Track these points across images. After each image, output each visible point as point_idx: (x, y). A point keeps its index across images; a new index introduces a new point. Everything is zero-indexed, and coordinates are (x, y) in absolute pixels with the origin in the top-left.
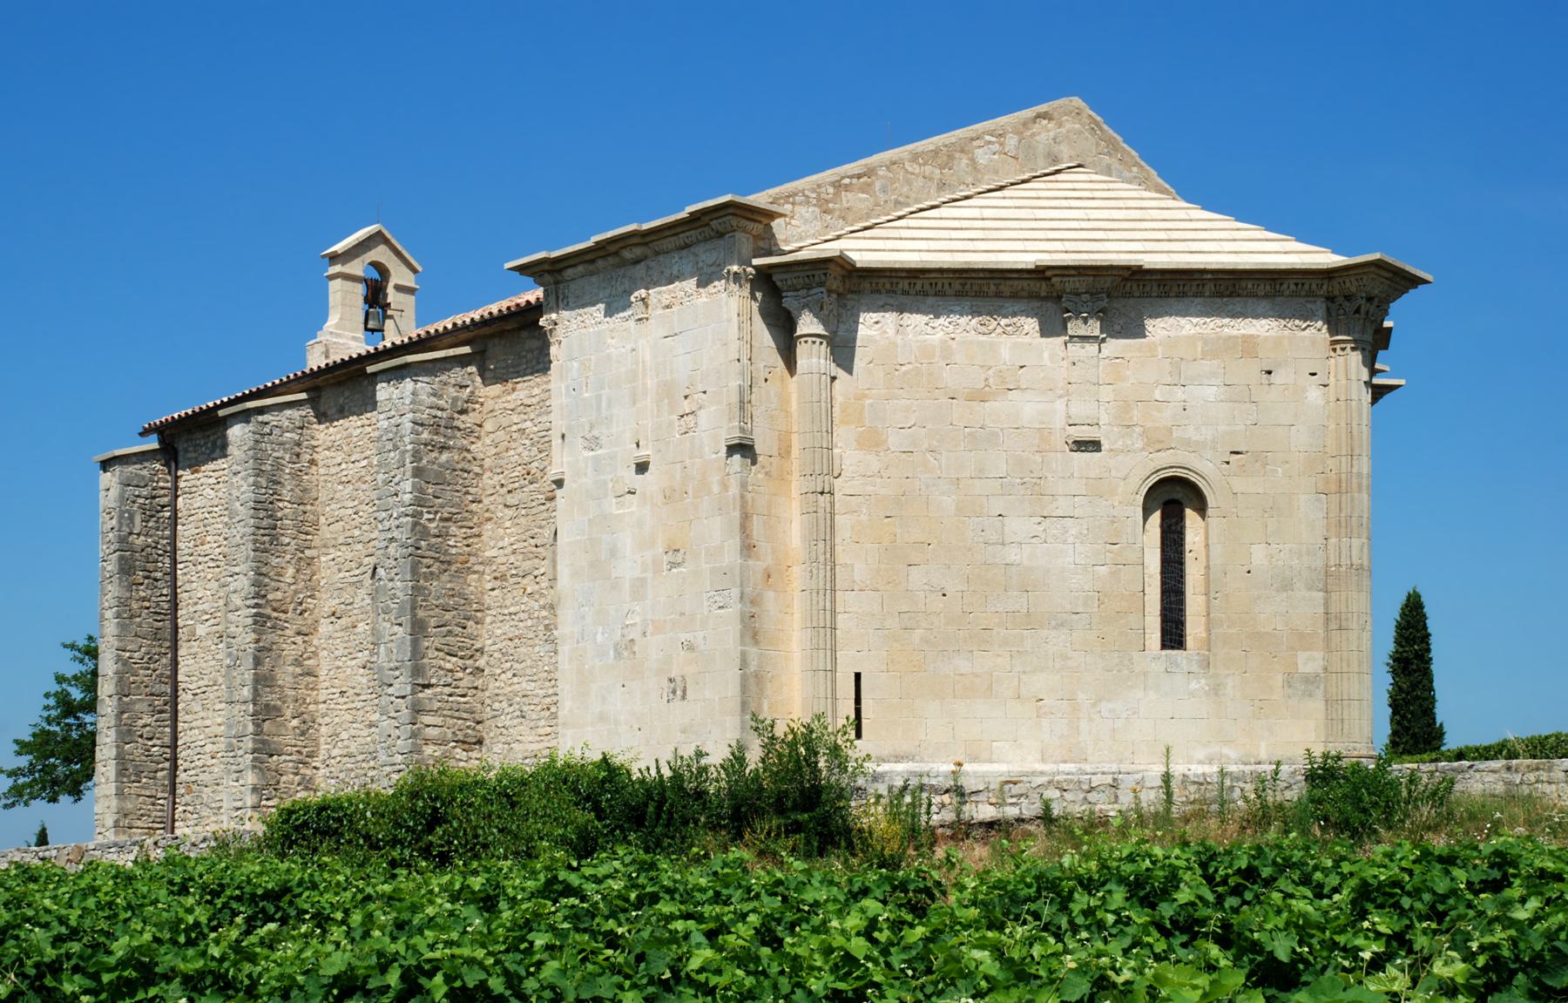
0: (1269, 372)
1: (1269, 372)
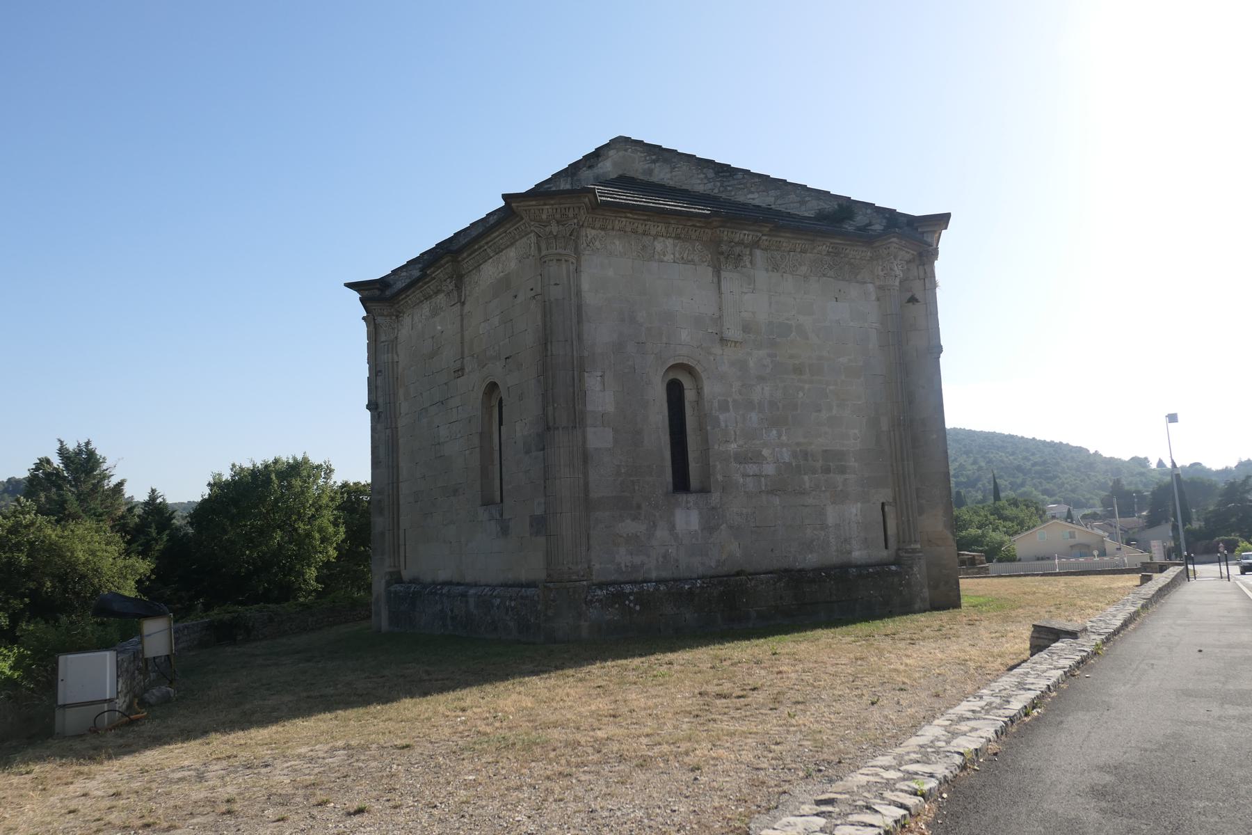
1: (516, 297)
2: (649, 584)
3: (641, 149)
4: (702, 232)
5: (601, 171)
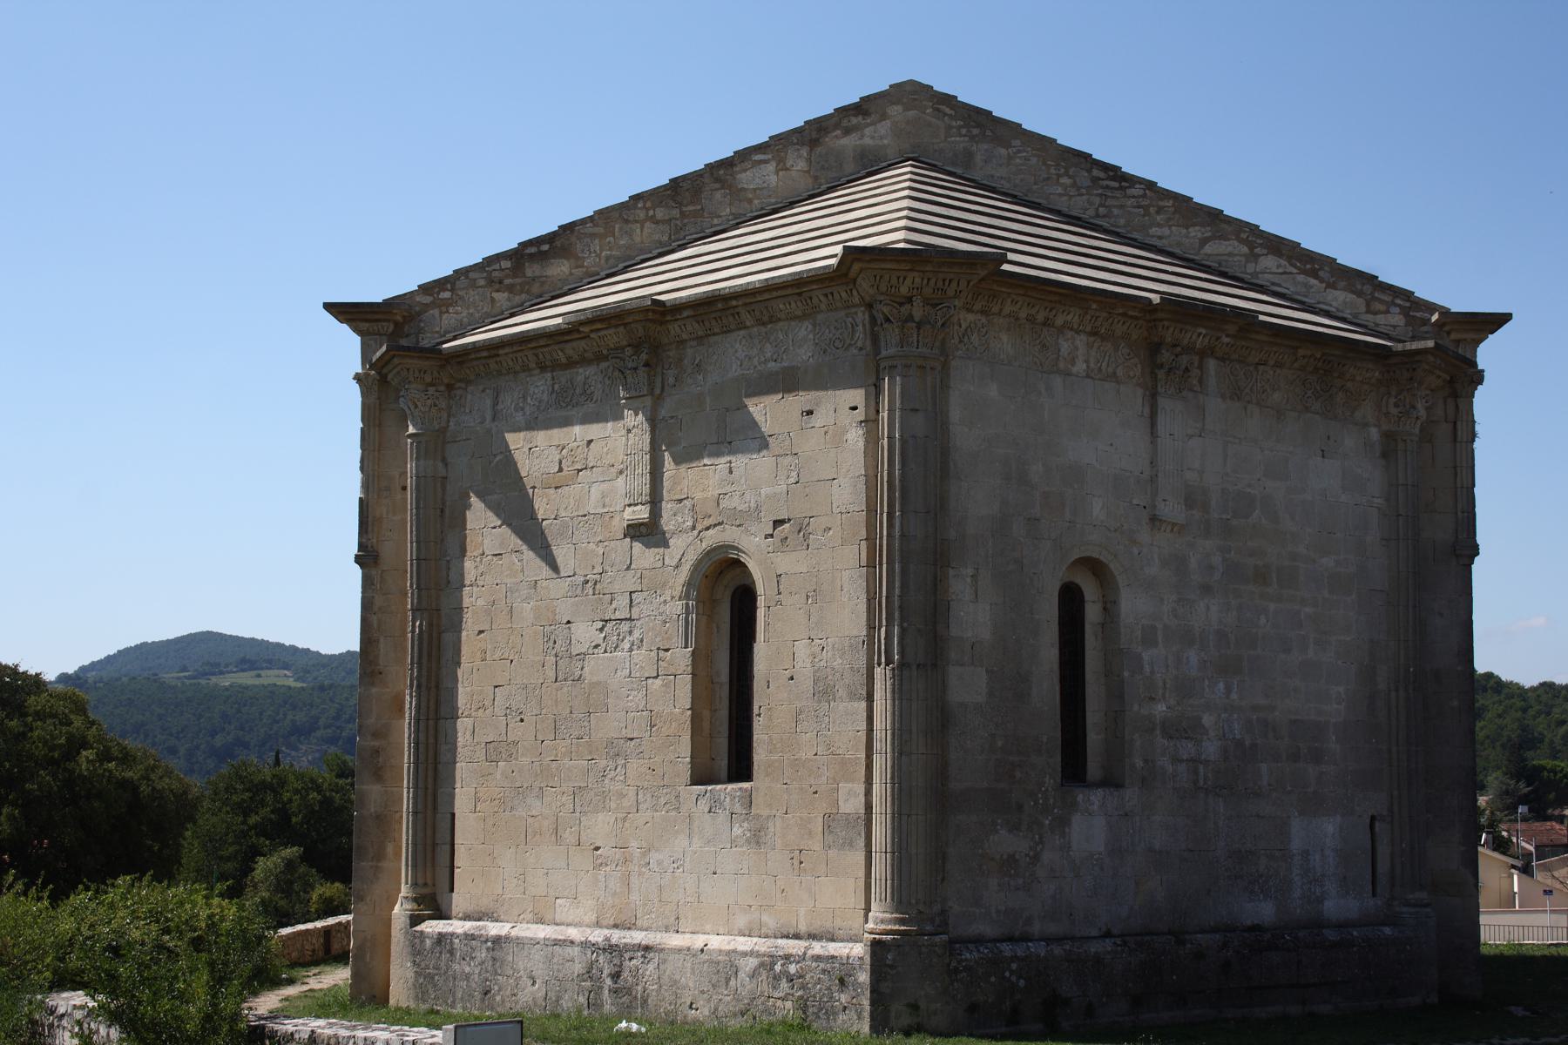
0: (810, 413)
1: (810, 413)
2: (1030, 944)
3: (953, 112)
4: (1133, 325)
5: (867, 141)
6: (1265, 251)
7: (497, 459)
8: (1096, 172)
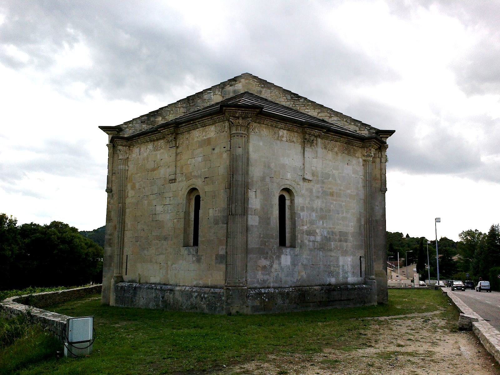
1: (214, 149)
3: (257, 81)
5: (236, 88)
6: (334, 115)
7: (140, 165)
8: (292, 96)
